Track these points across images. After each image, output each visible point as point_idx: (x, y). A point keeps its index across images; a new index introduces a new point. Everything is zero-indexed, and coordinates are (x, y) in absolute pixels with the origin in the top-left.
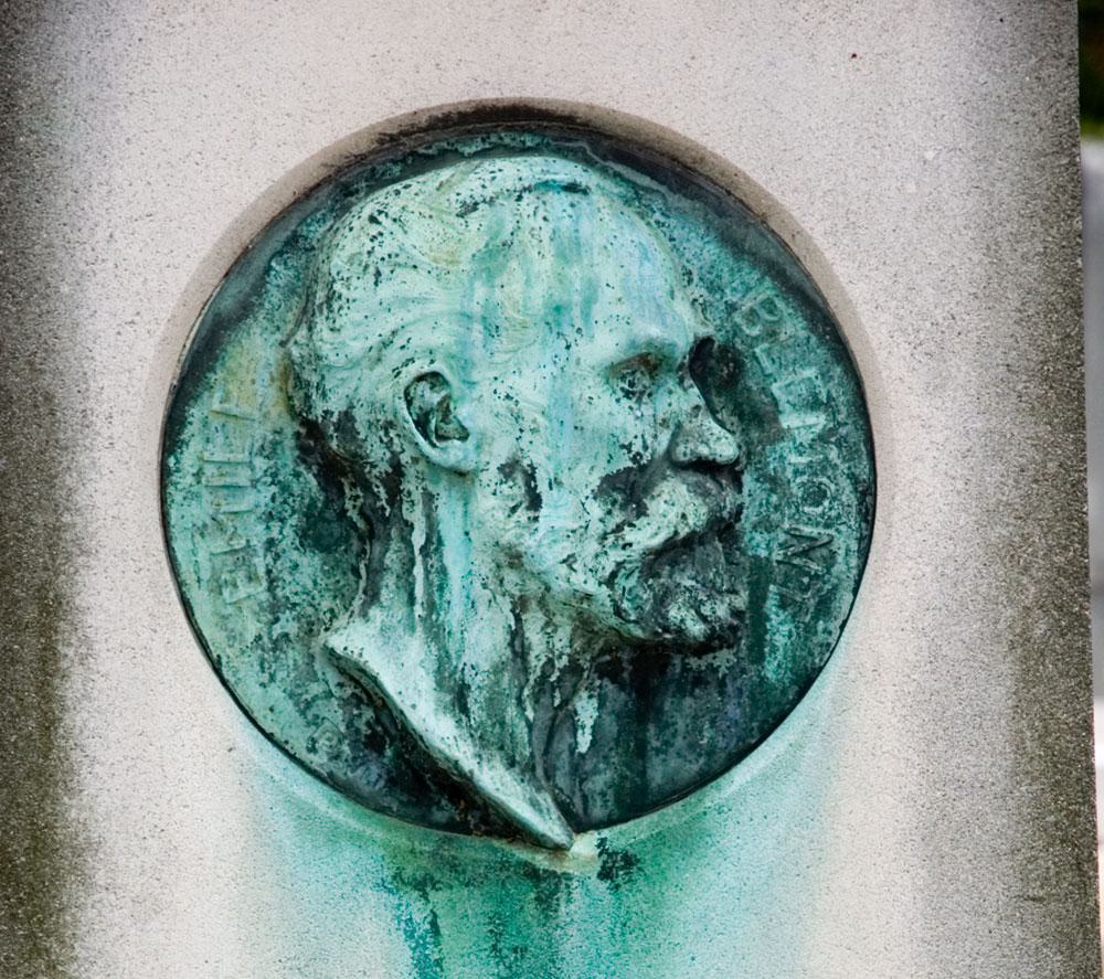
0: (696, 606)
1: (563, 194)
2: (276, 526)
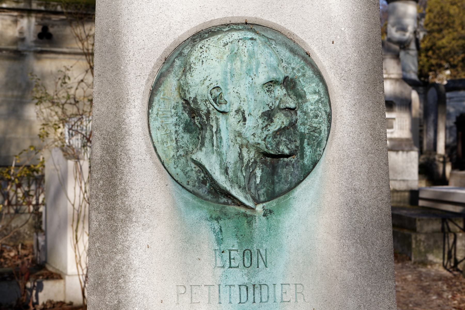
0: (286, 145)
2: (177, 127)
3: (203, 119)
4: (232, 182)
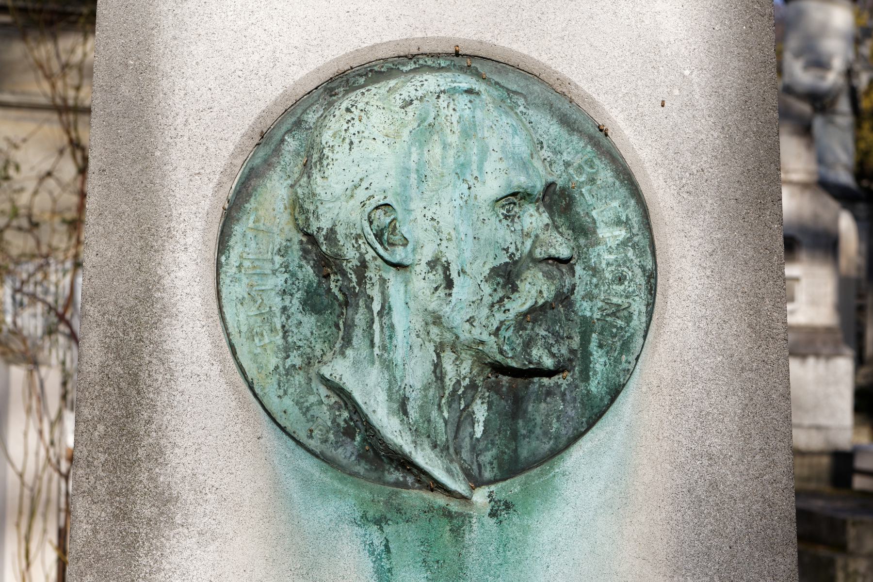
0: (548, 347)
1: (465, 95)
2: (287, 298)
3: (350, 281)
4: (416, 432)
